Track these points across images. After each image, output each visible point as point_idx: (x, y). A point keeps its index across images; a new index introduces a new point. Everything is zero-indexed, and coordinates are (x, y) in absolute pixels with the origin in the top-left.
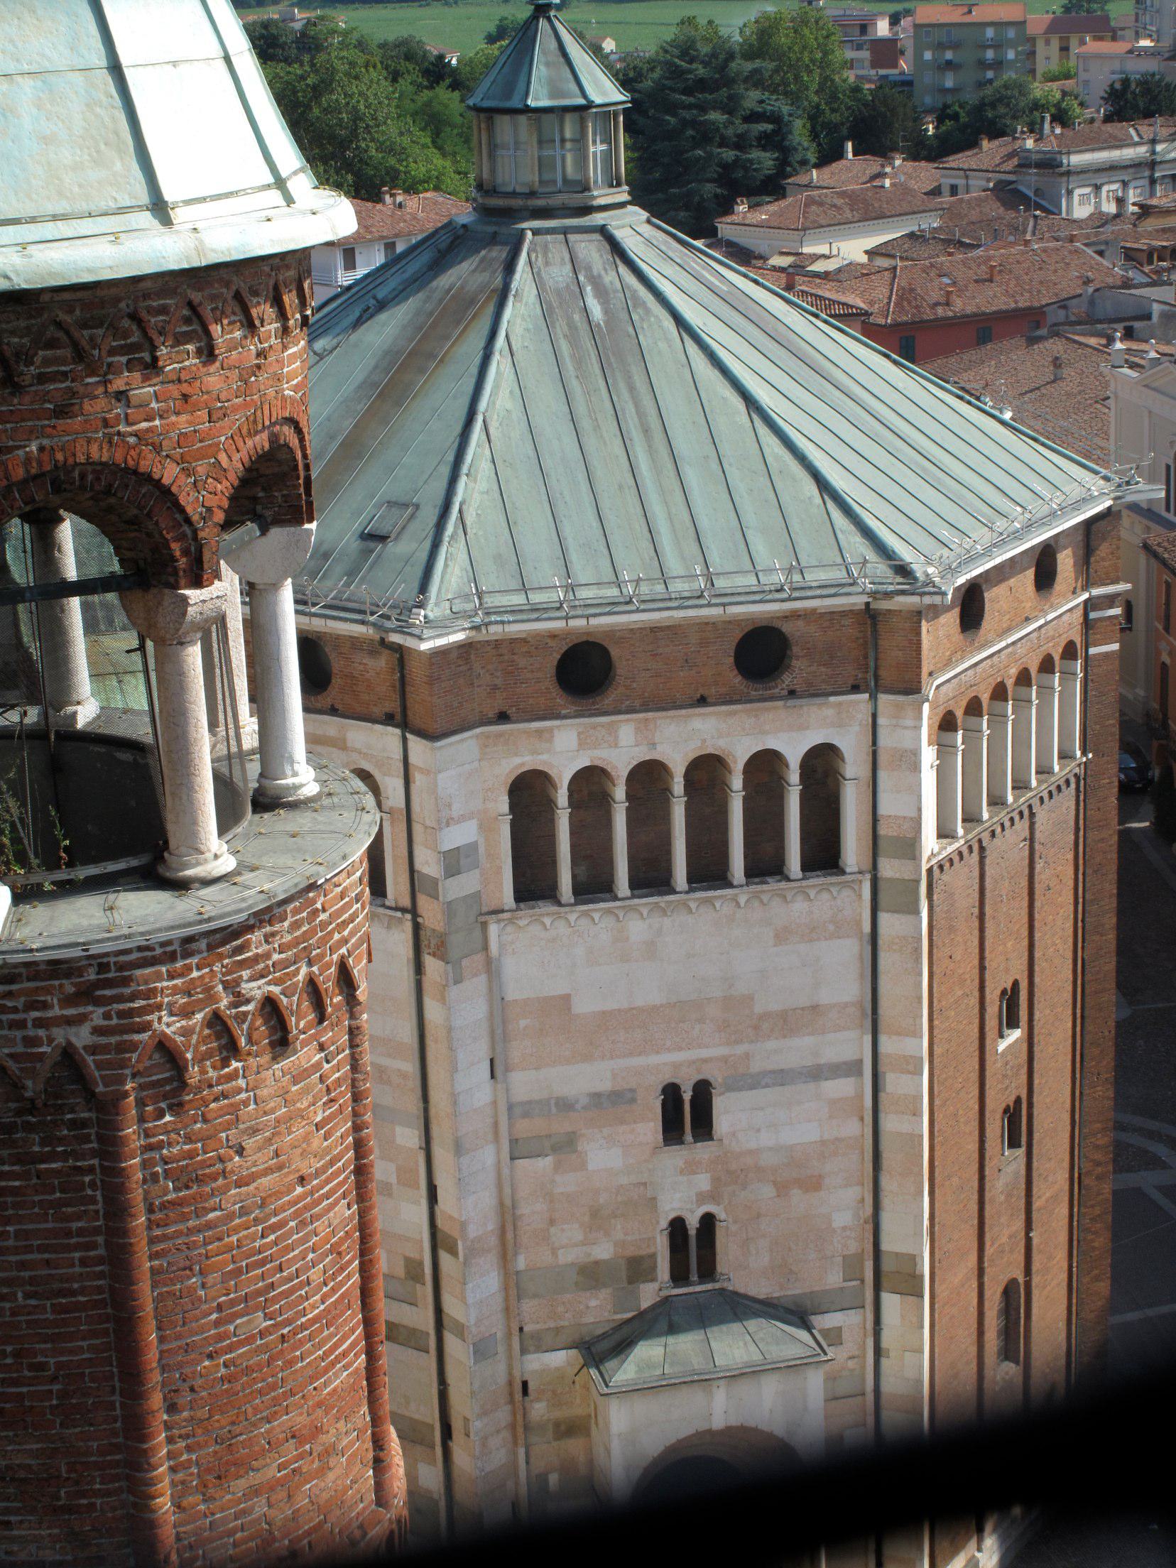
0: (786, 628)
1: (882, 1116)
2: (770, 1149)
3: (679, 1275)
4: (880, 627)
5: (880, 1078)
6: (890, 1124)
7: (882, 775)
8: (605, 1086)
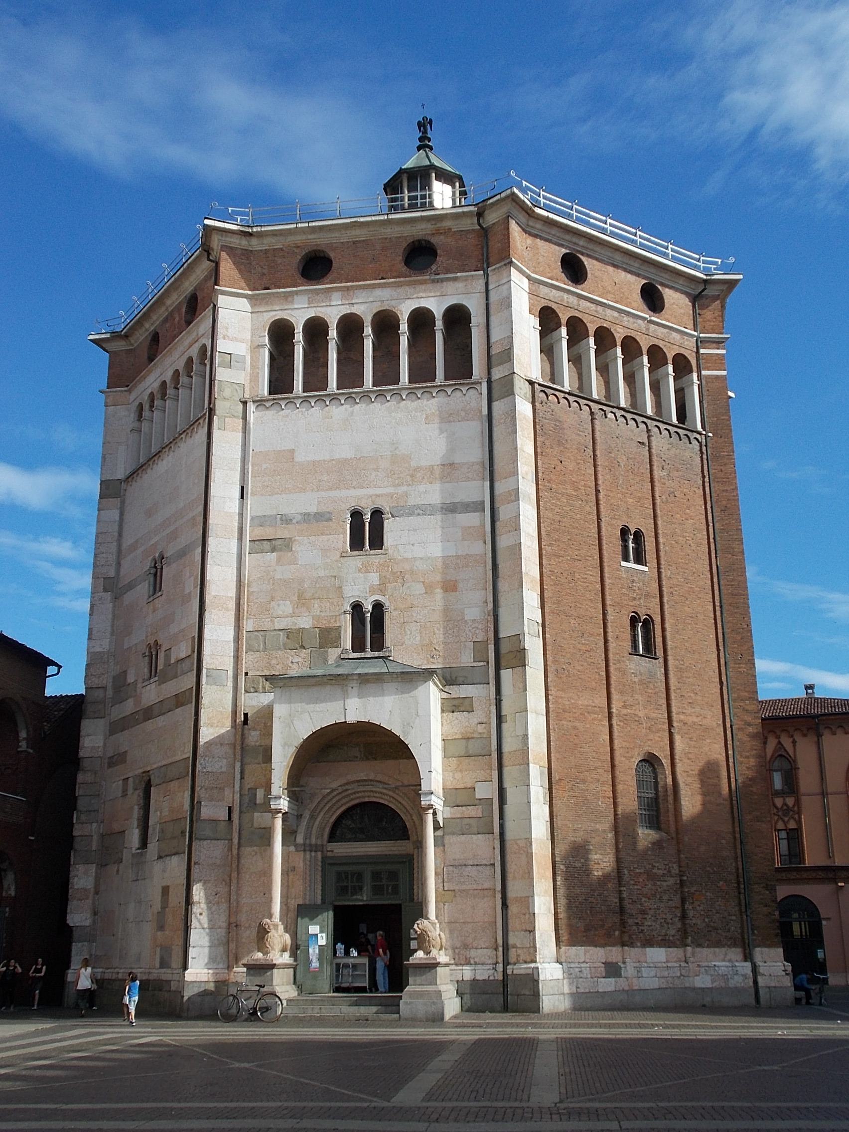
0: (434, 240)
1: (498, 538)
2: (421, 559)
3: (357, 645)
4: (489, 236)
5: (496, 512)
6: (503, 542)
7: (493, 319)
8: (313, 509)
